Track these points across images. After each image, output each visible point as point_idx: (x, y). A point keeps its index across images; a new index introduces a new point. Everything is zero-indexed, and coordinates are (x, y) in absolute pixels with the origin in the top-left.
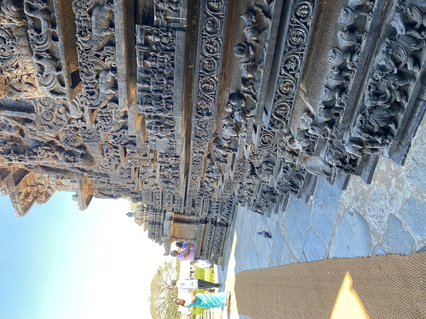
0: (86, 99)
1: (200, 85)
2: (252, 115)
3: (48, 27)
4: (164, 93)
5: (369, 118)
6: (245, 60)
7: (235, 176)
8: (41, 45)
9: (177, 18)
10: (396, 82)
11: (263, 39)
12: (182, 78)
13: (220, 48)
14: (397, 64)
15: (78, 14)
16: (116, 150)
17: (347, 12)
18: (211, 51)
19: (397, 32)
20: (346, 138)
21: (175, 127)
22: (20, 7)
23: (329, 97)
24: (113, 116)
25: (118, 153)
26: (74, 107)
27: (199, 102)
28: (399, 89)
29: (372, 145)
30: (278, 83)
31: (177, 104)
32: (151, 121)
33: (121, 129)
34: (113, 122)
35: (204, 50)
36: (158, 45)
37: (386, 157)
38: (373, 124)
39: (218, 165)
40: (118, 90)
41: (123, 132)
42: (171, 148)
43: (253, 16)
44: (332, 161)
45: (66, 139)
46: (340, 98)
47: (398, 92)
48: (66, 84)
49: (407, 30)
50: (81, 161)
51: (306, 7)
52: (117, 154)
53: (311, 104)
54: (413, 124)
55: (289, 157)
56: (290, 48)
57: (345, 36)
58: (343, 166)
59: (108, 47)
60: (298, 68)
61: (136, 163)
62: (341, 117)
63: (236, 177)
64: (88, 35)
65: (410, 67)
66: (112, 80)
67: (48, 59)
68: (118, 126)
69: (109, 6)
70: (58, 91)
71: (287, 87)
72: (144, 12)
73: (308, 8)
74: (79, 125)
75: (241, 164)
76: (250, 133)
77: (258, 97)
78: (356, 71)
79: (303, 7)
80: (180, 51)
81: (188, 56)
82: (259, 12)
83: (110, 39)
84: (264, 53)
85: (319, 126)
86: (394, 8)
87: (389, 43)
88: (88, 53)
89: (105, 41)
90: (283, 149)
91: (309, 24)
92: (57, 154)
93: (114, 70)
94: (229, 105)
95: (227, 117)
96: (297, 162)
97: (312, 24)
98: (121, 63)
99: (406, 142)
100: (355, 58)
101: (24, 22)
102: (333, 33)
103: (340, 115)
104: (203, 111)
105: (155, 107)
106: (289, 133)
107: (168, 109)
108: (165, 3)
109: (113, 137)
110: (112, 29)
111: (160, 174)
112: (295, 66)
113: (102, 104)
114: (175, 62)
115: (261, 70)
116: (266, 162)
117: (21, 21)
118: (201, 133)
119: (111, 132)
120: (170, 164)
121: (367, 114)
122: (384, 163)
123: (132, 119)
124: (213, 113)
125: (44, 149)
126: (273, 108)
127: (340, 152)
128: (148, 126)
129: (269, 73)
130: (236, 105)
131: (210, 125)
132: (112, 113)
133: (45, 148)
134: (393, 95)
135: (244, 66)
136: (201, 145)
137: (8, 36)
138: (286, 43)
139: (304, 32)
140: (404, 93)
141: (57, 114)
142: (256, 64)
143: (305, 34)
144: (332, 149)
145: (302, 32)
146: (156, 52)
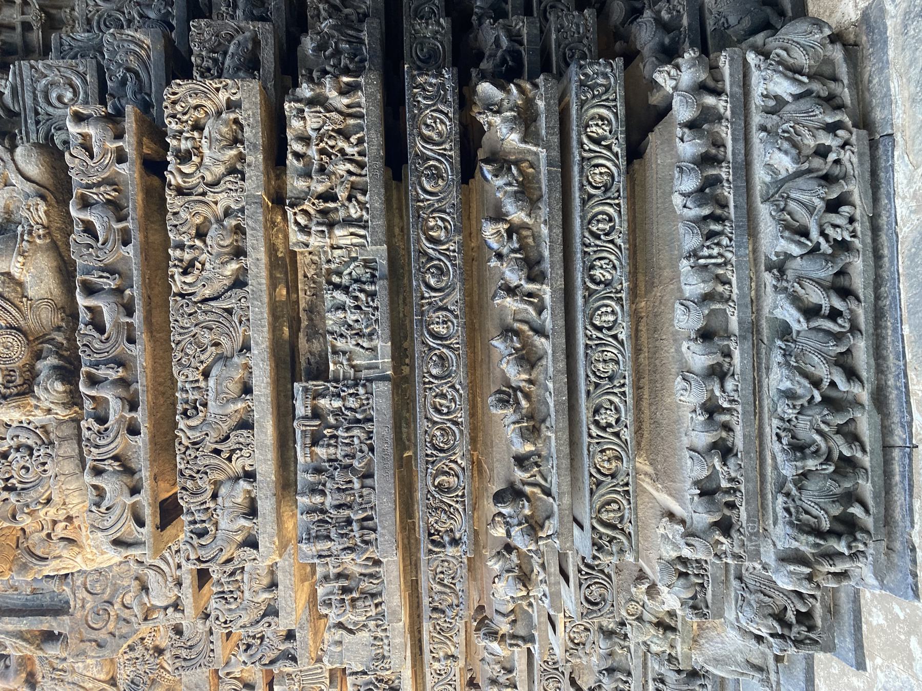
0: (188, 546)
1: (430, 480)
2: (550, 533)
4: (356, 508)
5: (801, 500)
6: (514, 418)
8: (104, 446)
10: (828, 418)
11: (542, 377)
12: (392, 472)
14: (816, 383)
15: (183, 377)
17: (687, 307)
18: (445, 410)
19: (791, 329)
20: (769, 556)
22: (70, 383)
23: (702, 469)
24: (245, 588)
26: (160, 579)
28: (839, 430)
29: (831, 562)
30: (589, 455)
31: (384, 528)
32: (328, 586)
33: (264, 616)
35: (431, 410)
36: (338, 415)
37: (873, 587)
38: (815, 512)
43: (515, 338)
44: (758, 624)
46: (725, 468)
47: (838, 436)
49: (808, 320)
51: (609, 309)
53: (670, 495)
54: (899, 497)
55: (658, 636)
56: (597, 386)
57: (697, 347)
58: (786, 632)
59: (239, 432)
60: (623, 419)
62: (742, 509)
64: (201, 414)
65: (842, 385)
67: (115, 472)
69: (241, 357)
70: (130, 540)
71: (609, 460)
72: (309, 363)
73: (613, 311)
74: (168, 620)
76: (554, 584)
77: (554, 490)
78: (739, 408)
79: (604, 309)
80: (383, 419)
81: (401, 432)
82: (524, 332)
83: (244, 417)
84: (549, 400)
85: (702, 535)
86: (769, 289)
87: (784, 347)
88: (197, 449)
89: (233, 422)
90: (640, 619)
91: (622, 337)
93: (250, 476)
94: (497, 519)
95: (498, 553)
96: (679, 648)
97: (629, 337)
98: (266, 460)
99: (902, 543)
100: (730, 384)
101: (76, 412)
102: (673, 350)
103: (738, 504)
104: (442, 537)
105: (337, 543)
106: (641, 576)
107: (367, 543)
110: (248, 397)
112: (616, 417)
114: (375, 441)
115: (549, 434)
116: (611, 671)
117: (70, 408)
121: (794, 492)
122: (875, 607)
124: (465, 539)
126: (591, 509)
127: (766, 599)
128: (324, 601)
129: (566, 436)
130: (512, 513)
134: (831, 444)
135: (514, 430)
137: (39, 442)
138: (587, 376)
139: (615, 351)
140: (854, 438)
142: (537, 426)
143: (619, 356)
144: (747, 595)
145: (612, 352)
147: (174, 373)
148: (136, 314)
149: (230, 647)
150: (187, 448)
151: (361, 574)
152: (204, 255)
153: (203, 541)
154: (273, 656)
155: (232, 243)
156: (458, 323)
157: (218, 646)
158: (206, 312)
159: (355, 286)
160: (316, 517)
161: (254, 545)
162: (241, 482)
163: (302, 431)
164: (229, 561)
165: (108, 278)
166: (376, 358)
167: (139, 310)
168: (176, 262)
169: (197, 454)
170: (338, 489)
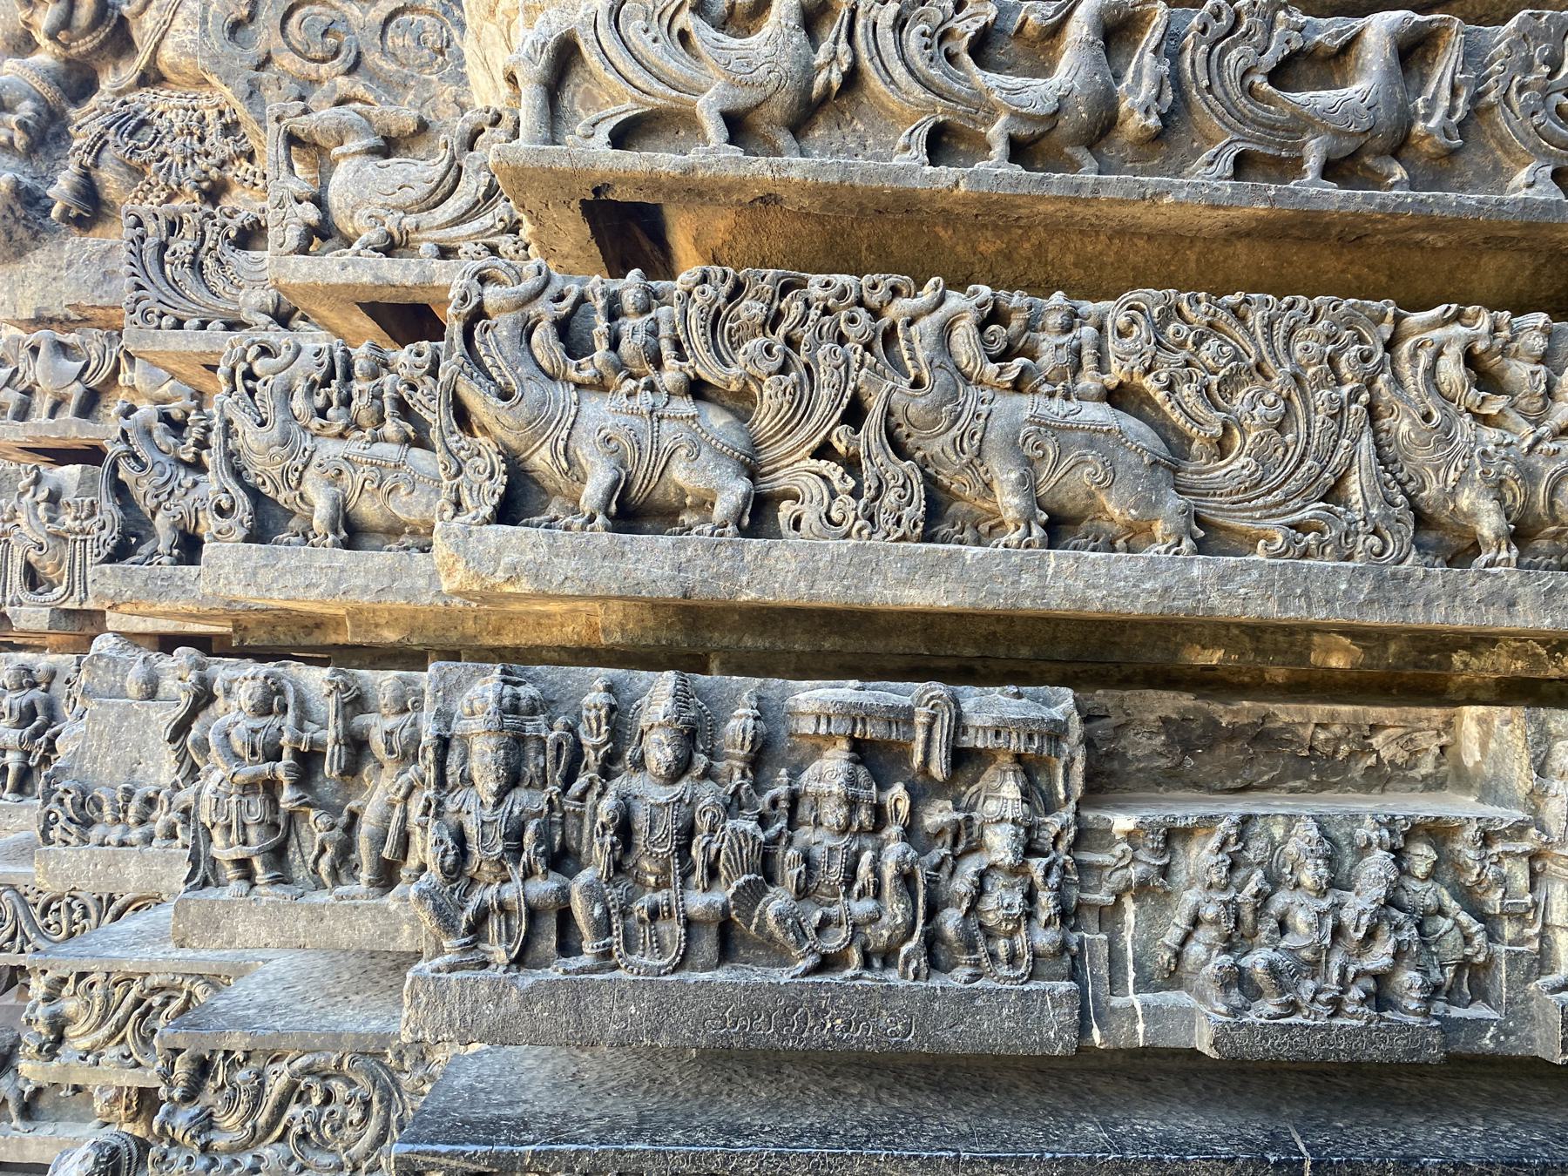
0: (531, 283)
3: (1014, 114)
4: (614, 894)
8: (900, 45)
9: (1132, 975)
15: (1122, 321)
16: (73, 402)
21: (279, 890)
24: (355, 446)
25: (52, 414)
31: (527, 999)
32: (327, 707)
33: (255, 494)
34: (308, 444)
36: (955, 842)
40: (607, 529)
41: (225, 504)
42: (90, 810)
48: (634, 161)
52: (42, 404)
59: (919, 491)
64: (992, 368)
66: (682, 492)
67: (810, 72)
68: (276, 473)
69: (1182, 521)
70: (572, 96)
74: (280, 204)
80: (940, 1017)
88: (868, 347)
92: (46, 56)
98: (812, 574)
105: (487, 814)
107: (477, 927)
108: (1225, 897)
109: (177, 414)
110: (1037, 532)
113: (493, 401)
118: (231, 1101)
119: (229, 422)
123: (337, 583)
128: (280, 691)
132: (375, 440)
136: (119, 1029)
141: (334, 90)
146: (909, 833)
147: (1139, 293)
148: (1335, 193)
150: (876, 314)
151: (354, 816)
152: (1527, 428)
153: (543, 336)
154: (138, 493)
155: (1555, 520)
157: (191, 341)
158: (1338, 416)
159: (1409, 933)
160: (593, 741)
161: (508, 511)
162: (742, 486)
163: (907, 716)
164: (462, 415)
165: (1450, 113)
166: (1143, 984)
167: (1346, 199)
168: (1506, 333)
169: (854, 348)
170: (689, 831)
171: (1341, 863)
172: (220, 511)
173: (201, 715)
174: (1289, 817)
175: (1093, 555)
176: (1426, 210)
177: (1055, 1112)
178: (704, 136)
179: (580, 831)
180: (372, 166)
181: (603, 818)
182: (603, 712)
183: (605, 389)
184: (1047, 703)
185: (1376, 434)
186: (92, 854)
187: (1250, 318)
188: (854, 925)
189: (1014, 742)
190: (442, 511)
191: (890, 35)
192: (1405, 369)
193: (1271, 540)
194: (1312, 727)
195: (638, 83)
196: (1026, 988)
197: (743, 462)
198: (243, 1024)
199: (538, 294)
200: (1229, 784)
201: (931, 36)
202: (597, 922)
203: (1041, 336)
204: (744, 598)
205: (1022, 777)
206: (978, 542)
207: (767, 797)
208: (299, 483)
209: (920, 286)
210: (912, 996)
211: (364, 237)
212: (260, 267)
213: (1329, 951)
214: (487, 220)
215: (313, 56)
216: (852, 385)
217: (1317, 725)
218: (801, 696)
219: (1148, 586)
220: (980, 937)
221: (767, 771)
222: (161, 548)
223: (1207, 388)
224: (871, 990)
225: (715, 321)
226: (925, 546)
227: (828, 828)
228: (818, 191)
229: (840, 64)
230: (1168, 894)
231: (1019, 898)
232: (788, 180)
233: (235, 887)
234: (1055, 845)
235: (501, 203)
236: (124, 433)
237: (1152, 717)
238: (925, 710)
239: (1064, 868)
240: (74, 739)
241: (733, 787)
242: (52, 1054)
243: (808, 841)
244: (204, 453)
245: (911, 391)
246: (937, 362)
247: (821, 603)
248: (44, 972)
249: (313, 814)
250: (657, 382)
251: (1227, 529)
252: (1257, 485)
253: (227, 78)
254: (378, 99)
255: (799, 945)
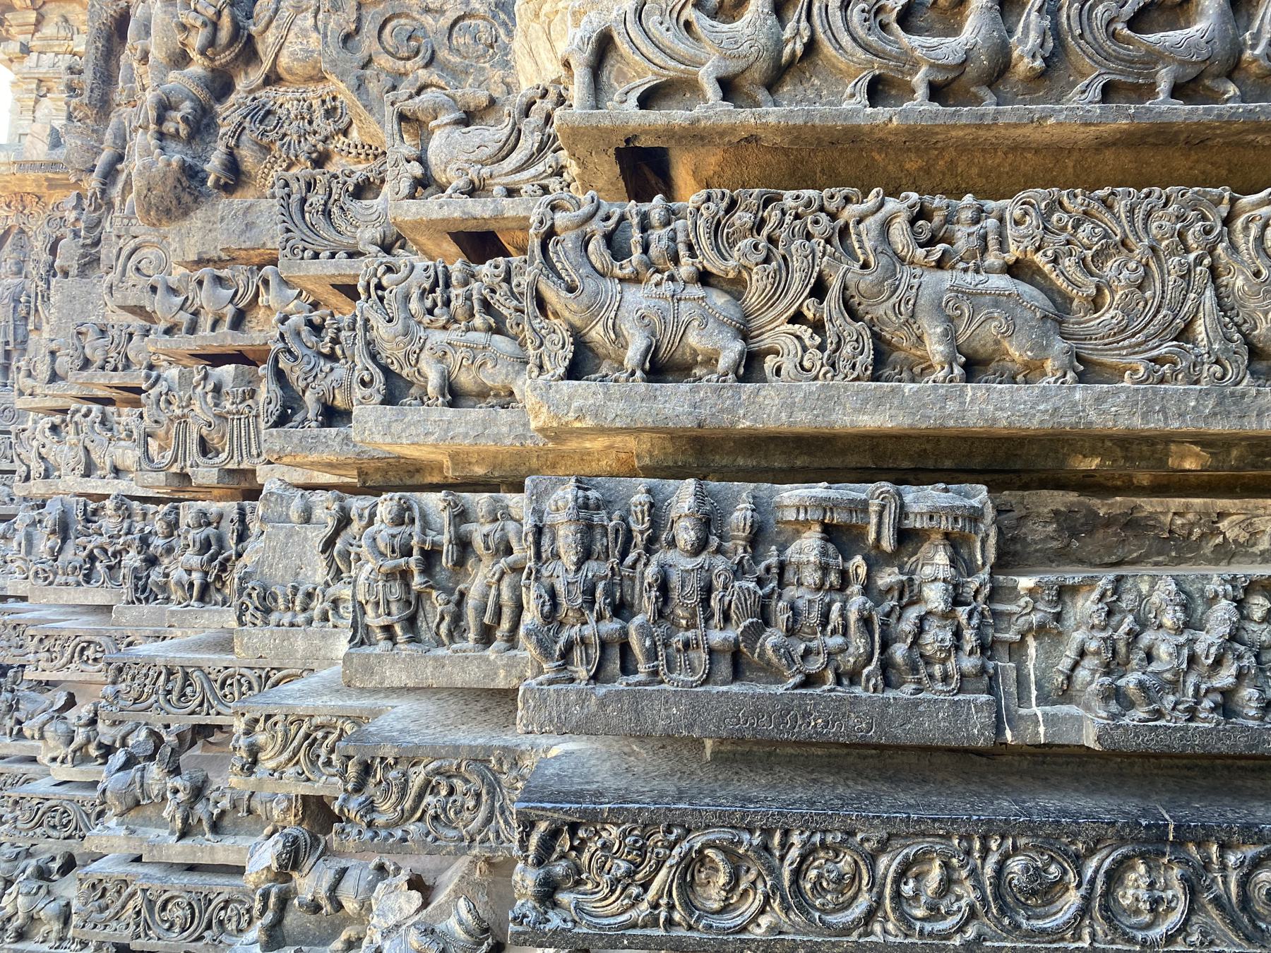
0: (587, 209)
3: (932, 66)
4: (658, 632)
7: (109, 885)
13: (930, 934)
15: (1017, 213)
16: (228, 319)
18: (908, 889)
21: (413, 646)
24: (454, 335)
25: (213, 329)
26: (488, 151)
27: (625, 835)
31: (602, 703)
33: (386, 370)
34: (422, 334)
35: (911, 851)
39: (169, 795)
41: (367, 378)
42: (269, 600)
45: (269, 112)
48: (656, 117)
50: (169, 165)
52: (206, 321)
59: (869, 344)
61: (162, 405)
63: (105, 889)
64: (921, 252)
66: (695, 353)
67: (780, 44)
68: (401, 355)
69: (1066, 359)
70: (608, 74)
74: (396, 164)
75: (177, 914)
80: (892, 719)
88: (828, 241)
92: (198, 67)
98: (790, 407)
104: (563, 856)
107: (566, 654)
108: (1104, 635)
110: (958, 370)
111: (107, 497)
113: (563, 293)
118: (387, 791)
119: (367, 320)
120: (166, 561)
123: (447, 431)
125: (219, 14)
128: (409, 509)
131: (436, 839)
132: (468, 330)
133: (226, 21)
136: (295, 754)
146: (867, 590)
147: (1030, 192)
148: (1181, 108)
149: (319, 290)
150: (833, 217)
151: (462, 595)
153: (596, 247)
154: (292, 377)
156: (1154, 944)
158: (1186, 276)
159: (1249, 661)
160: (639, 527)
161: (574, 371)
162: (738, 346)
163: (863, 507)
164: (541, 303)
166: (1043, 700)
169: (818, 243)
170: (708, 590)
171: (1195, 610)
172: (363, 383)
173: (342, 534)
174: (1153, 577)
175: (1000, 386)
176: (1255, 117)
177: (978, 794)
178: (704, 97)
179: (633, 590)
180: (458, 132)
181: (649, 578)
182: (646, 508)
183: (640, 282)
184: (967, 496)
185: (1217, 289)
186: (272, 632)
187: (1116, 205)
188: (829, 654)
189: (944, 522)
190: (531, 372)
191: (838, 13)
192: (1239, 238)
193: (1135, 371)
194: (1170, 515)
195: (656, 61)
196: (956, 698)
197: (738, 329)
198: (392, 740)
199: (591, 216)
200: (1106, 560)
201: (869, 12)
202: (647, 650)
203: (957, 227)
204: (741, 426)
205: (949, 549)
206: (913, 381)
207: (763, 565)
208: (417, 362)
209: (866, 195)
210: (873, 703)
211: (454, 184)
212: (371, 211)
213: (1186, 673)
214: (540, 167)
215: (400, 55)
216: (817, 269)
217: (1175, 514)
218: (785, 495)
219: (1042, 407)
220: (921, 663)
221: (761, 549)
222: (310, 416)
223: (1084, 260)
224: (841, 699)
225: (717, 228)
226: (874, 384)
227: (808, 587)
228: (788, 130)
229: (802, 38)
230: (1060, 633)
231: (949, 635)
232: (766, 124)
233: (383, 645)
234: (975, 597)
235: (550, 155)
236: (282, 335)
237: (1046, 511)
238: (877, 501)
239: (982, 613)
240: (257, 552)
241: (738, 559)
242: (250, 771)
243: (793, 596)
244: (337, 347)
245: (861, 271)
246: (880, 249)
247: (798, 429)
248: (243, 715)
249: (434, 594)
250: (676, 273)
251: (1101, 364)
252: (1123, 331)
253: (342, 77)
254: (448, 84)
255: (789, 668)
